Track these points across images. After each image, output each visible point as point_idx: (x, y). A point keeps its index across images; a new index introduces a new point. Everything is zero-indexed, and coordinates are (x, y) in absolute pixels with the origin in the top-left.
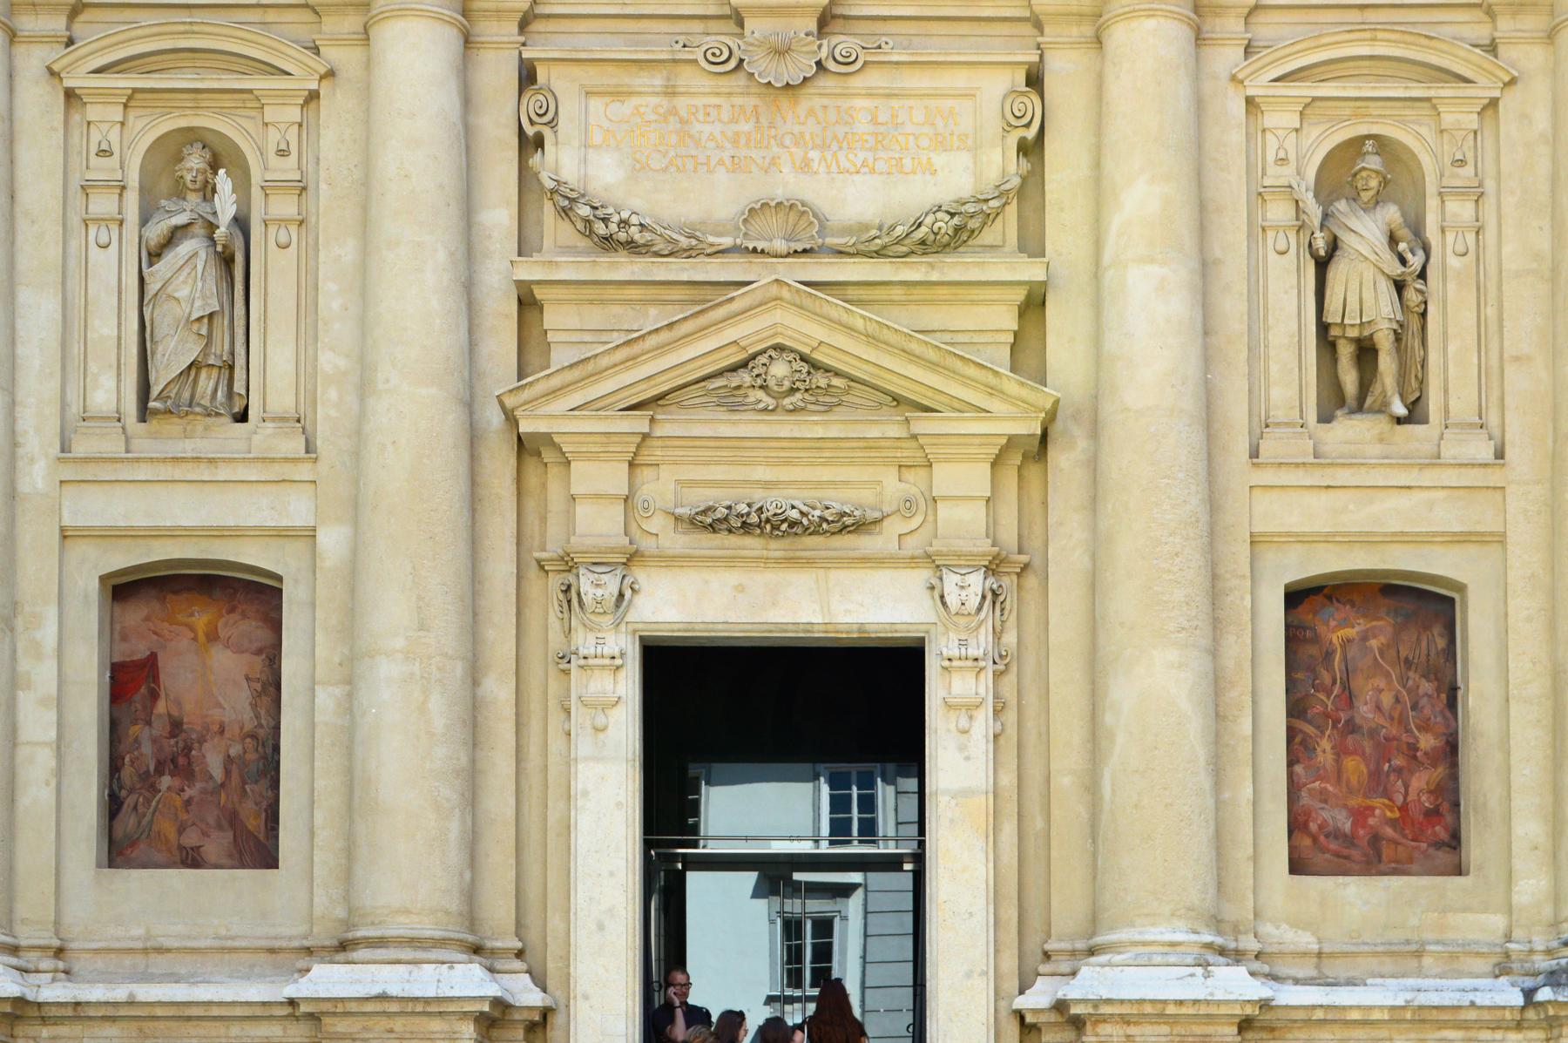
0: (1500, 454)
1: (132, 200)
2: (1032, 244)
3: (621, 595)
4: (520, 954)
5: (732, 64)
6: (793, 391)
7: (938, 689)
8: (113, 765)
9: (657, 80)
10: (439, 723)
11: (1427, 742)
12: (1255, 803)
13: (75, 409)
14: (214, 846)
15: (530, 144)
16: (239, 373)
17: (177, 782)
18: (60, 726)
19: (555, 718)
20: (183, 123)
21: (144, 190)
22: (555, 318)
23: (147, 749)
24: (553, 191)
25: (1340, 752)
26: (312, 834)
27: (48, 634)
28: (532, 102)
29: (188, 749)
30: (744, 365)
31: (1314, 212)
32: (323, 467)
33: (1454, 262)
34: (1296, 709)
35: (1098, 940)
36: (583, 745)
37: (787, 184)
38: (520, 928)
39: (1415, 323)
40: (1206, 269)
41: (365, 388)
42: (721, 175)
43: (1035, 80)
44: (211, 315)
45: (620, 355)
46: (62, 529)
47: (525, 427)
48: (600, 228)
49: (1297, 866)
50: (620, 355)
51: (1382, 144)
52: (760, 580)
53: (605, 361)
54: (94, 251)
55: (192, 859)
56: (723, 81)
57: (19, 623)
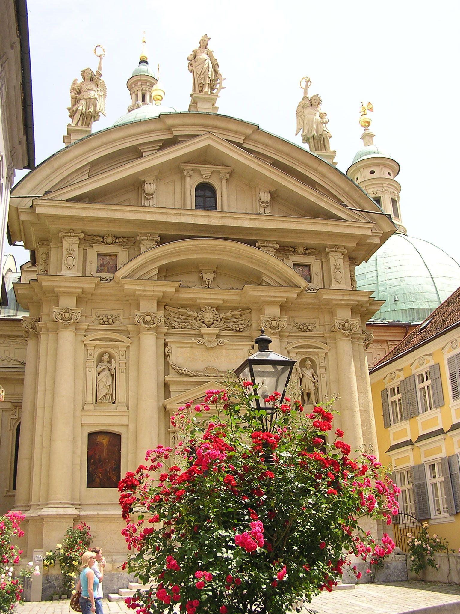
5: (202, 343)
9: (189, 345)
15: (166, 356)
20: (104, 350)
22: (171, 387)
37: (211, 364)
39: (316, 390)
48: (180, 371)
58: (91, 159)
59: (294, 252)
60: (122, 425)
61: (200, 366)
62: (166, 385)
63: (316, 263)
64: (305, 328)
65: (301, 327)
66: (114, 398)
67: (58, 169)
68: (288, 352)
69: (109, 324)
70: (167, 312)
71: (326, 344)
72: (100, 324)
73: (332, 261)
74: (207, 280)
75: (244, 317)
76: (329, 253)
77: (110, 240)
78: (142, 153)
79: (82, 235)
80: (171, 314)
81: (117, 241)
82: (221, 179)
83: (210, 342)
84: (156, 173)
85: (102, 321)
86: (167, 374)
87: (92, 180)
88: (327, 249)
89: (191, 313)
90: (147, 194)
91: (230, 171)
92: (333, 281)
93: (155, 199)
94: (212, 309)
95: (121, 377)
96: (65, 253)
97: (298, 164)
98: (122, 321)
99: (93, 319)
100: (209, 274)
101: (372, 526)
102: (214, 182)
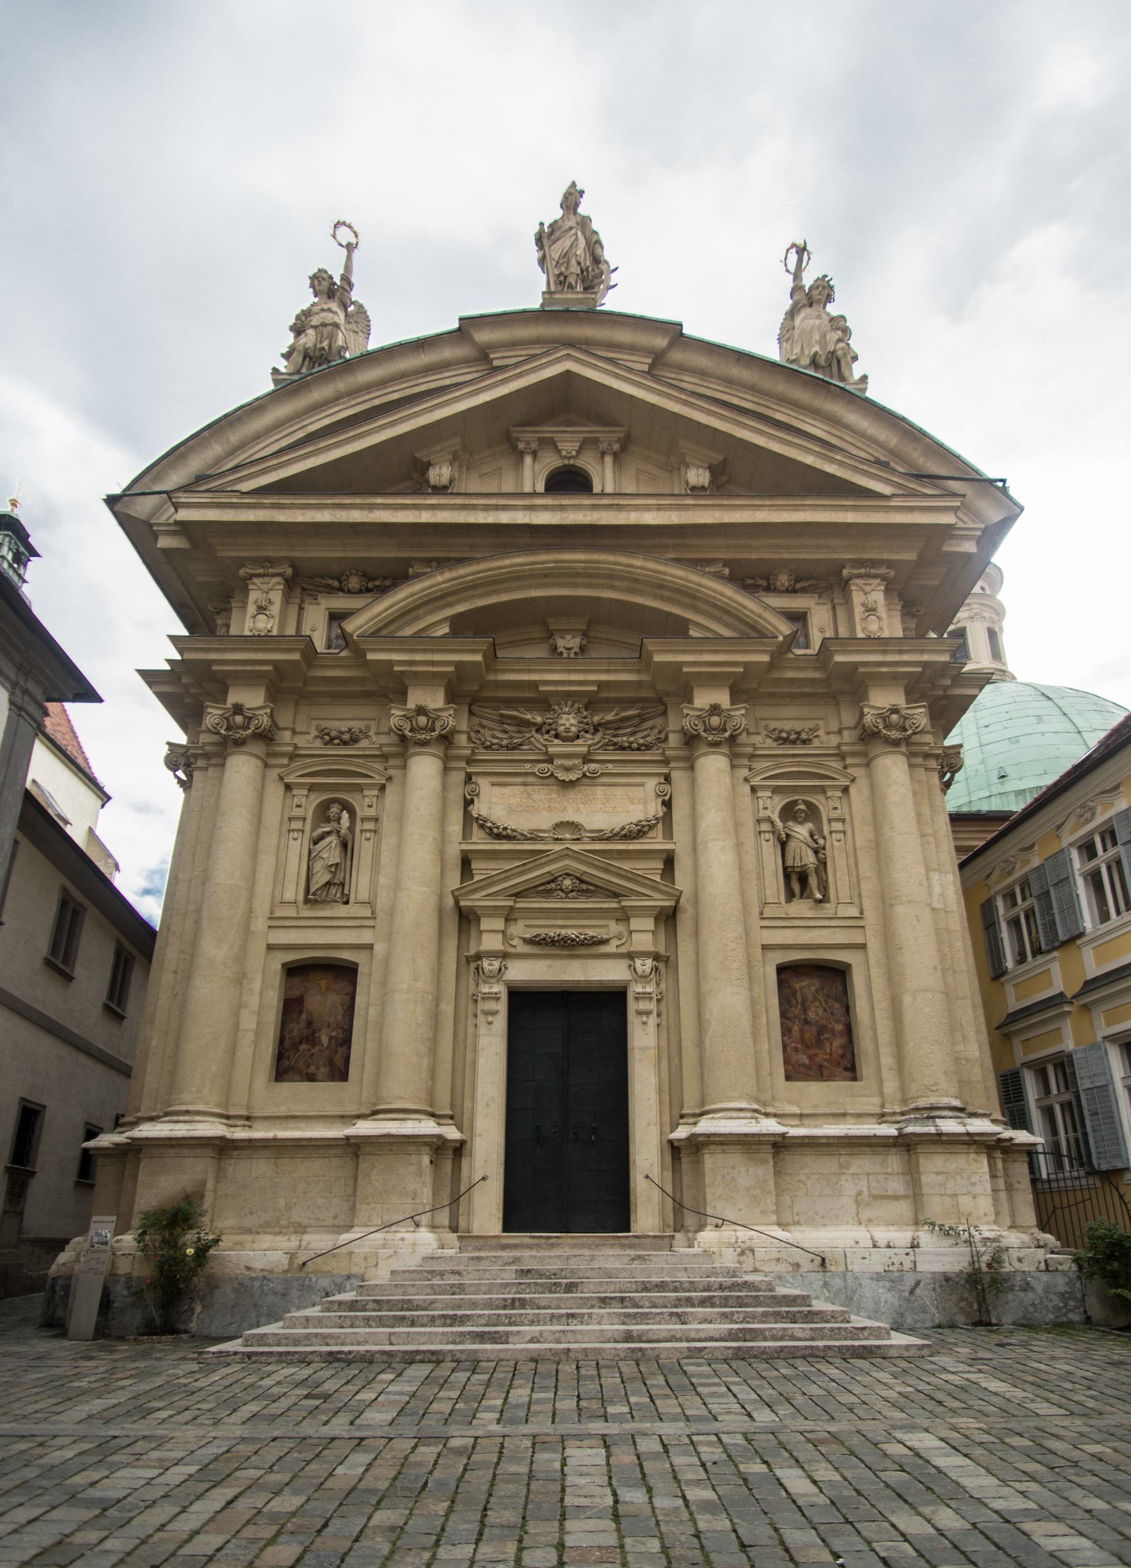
0: (862, 913)
1: (309, 822)
2: (669, 834)
3: (500, 970)
4: (452, 1117)
6: (572, 891)
7: (632, 1006)
8: (282, 1040)
9: (520, 780)
10: (421, 1019)
12: (770, 1051)
13: (278, 899)
15: (468, 803)
16: (347, 887)
17: (307, 1047)
18: (258, 1023)
19: (470, 1021)
20: (331, 796)
21: (313, 820)
23: (295, 1033)
24: (477, 819)
26: (363, 1066)
27: (257, 986)
28: (470, 787)
29: (314, 1033)
30: (553, 881)
32: (378, 920)
33: (836, 844)
34: (783, 1015)
35: (707, 1108)
36: (483, 1029)
37: (570, 816)
38: (452, 1106)
41: (397, 886)
42: (544, 813)
43: (667, 779)
44: (337, 865)
45: (502, 876)
46: (268, 945)
47: (462, 903)
48: (495, 831)
50: (502, 876)
52: (558, 964)
53: (496, 878)
54: (291, 841)
55: (311, 1078)
56: (546, 781)
57: (245, 981)
61: (543, 820)
62: (466, 862)
63: (819, 607)
64: (793, 736)
65: (784, 735)
66: (346, 892)
68: (753, 789)
69: (345, 743)
70: (476, 720)
72: (326, 744)
73: (857, 598)
74: (564, 651)
75: (650, 724)
76: (850, 579)
77: (354, 583)
80: (485, 722)
81: (370, 585)
82: (603, 454)
83: (567, 769)
85: (327, 738)
88: (845, 572)
89: (529, 716)
94: (576, 706)
95: (364, 849)
96: (251, 609)
97: (775, 407)
98: (374, 738)
99: (309, 738)
100: (568, 637)
101: (975, 1179)
102: (588, 463)
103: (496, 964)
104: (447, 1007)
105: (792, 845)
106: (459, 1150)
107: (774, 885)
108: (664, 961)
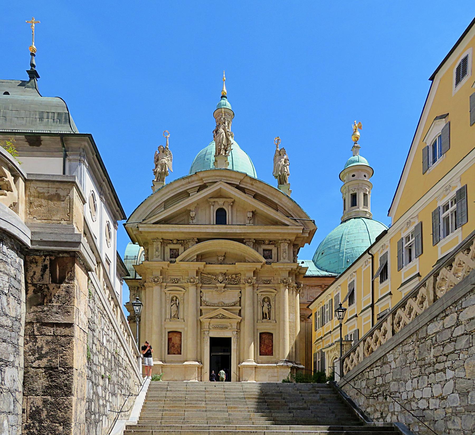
2: (240, 306)
11: (270, 345)
14: (176, 353)
15: (201, 297)
25: (264, 346)
28: (201, 294)
31: (262, 303)
34: (260, 342)
36: (205, 345)
40: (254, 307)
43: (241, 292)
49: (260, 355)
51: (268, 298)
58: (164, 200)
59: (264, 243)
60: (181, 328)
61: (216, 301)
62: (201, 310)
64: (266, 282)
67: (149, 206)
71: (276, 290)
73: (282, 248)
75: (237, 278)
78: (189, 194)
79: (162, 241)
84: (196, 205)
86: (201, 305)
87: (165, 211)
90: (191, 217)
91: (233, 201)
92: (282, 258)
93: (196, 219)
102: (224, 207)
103: (207, 332)
104: (199, 341)
105: (264, 308)
106: (201, 368)
107: (260, 316)
108: (239, 331)
